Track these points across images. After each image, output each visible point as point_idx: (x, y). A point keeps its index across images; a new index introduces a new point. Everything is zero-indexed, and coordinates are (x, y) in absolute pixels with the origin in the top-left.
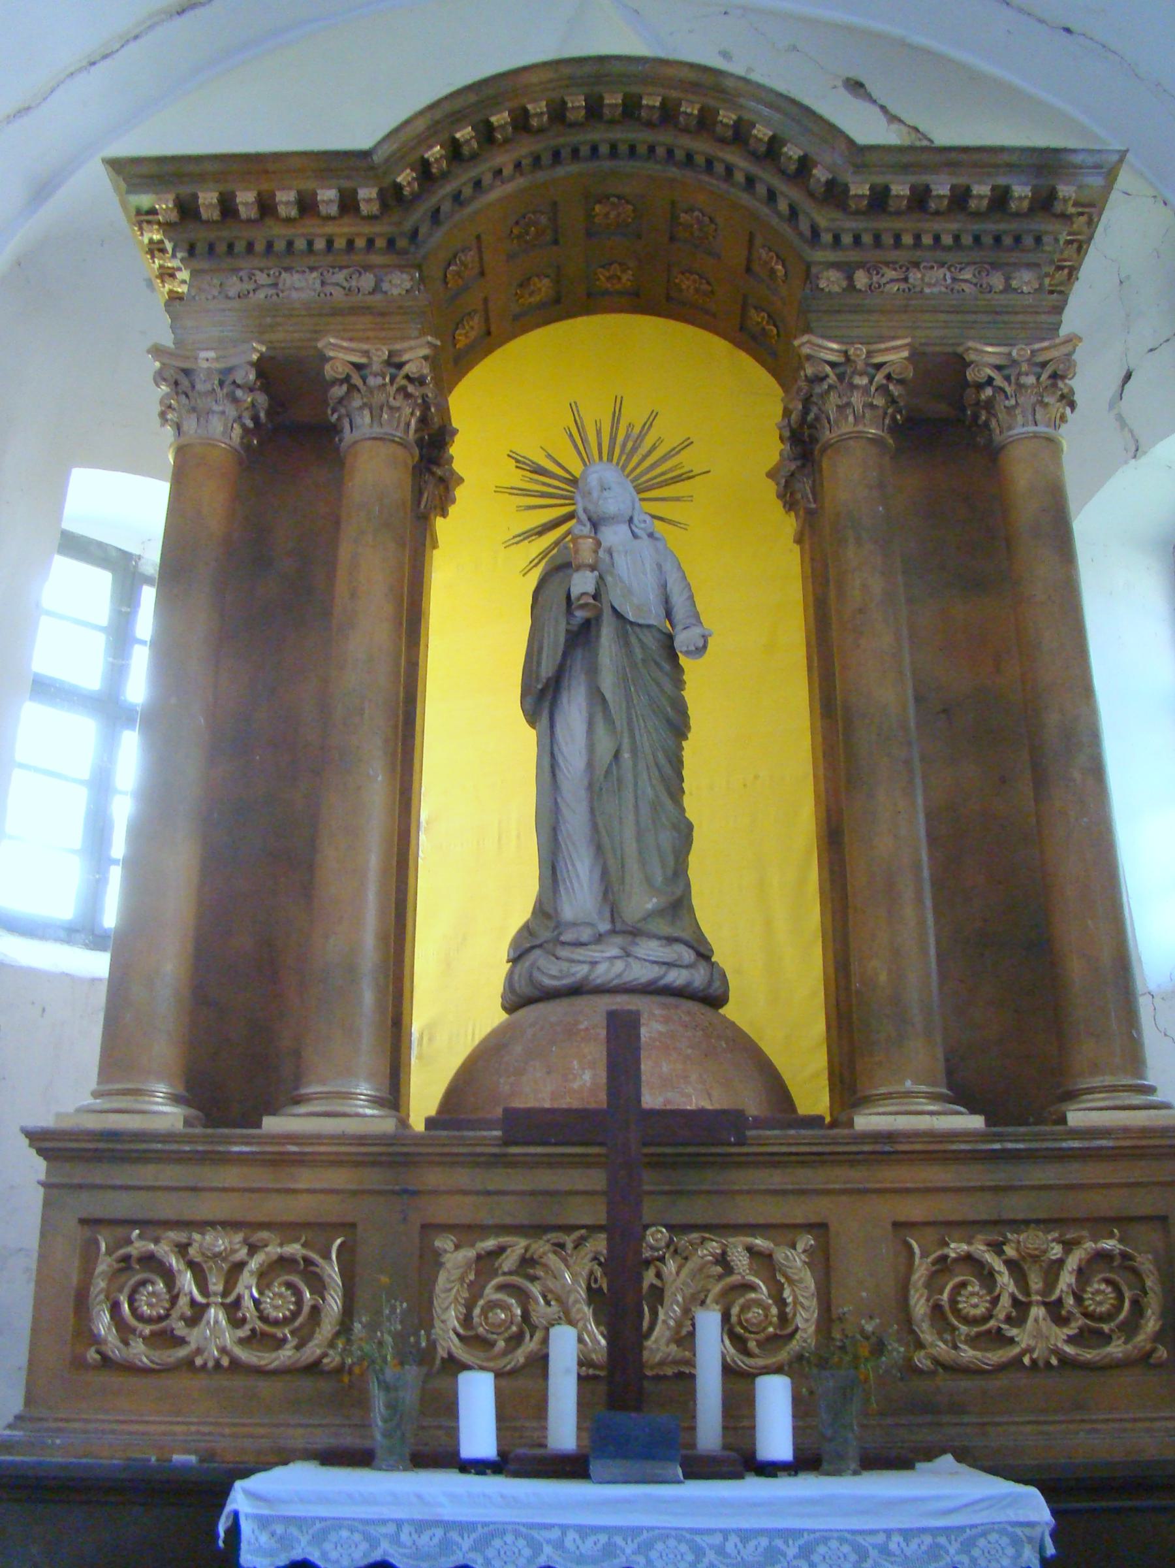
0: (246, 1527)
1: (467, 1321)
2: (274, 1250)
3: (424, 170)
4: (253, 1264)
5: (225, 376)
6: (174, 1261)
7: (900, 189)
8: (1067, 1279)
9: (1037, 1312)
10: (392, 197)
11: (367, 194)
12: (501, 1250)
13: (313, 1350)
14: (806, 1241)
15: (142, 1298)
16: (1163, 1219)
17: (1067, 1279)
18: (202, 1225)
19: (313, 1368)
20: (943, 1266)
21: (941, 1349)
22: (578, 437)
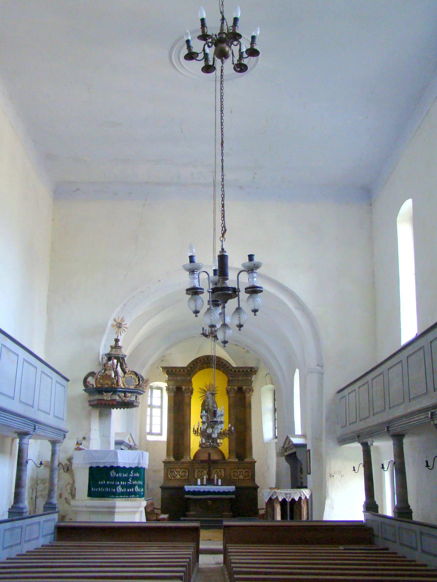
0: (186, 489)
1: (197, 475)
2: (182, 470)
3: (191, 367)
4: (181, 471)
5: (172, 389)
6: (175, 471)
7: (237, 371)
8: (244, 473)
9: (241, 475)
10: (188, 370)
11: (186, 371)
12: (200, 470)
13: (186, 478)
14: (224, 469)
15: (172, 474)
16: (251, 468)
17: (244, 473)
18: (177, 468)
19: (186, 479)
20: (234, 472)
21: (233, 478)
22: (206, 386)
